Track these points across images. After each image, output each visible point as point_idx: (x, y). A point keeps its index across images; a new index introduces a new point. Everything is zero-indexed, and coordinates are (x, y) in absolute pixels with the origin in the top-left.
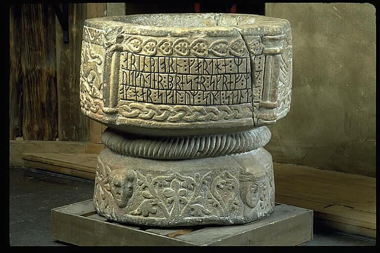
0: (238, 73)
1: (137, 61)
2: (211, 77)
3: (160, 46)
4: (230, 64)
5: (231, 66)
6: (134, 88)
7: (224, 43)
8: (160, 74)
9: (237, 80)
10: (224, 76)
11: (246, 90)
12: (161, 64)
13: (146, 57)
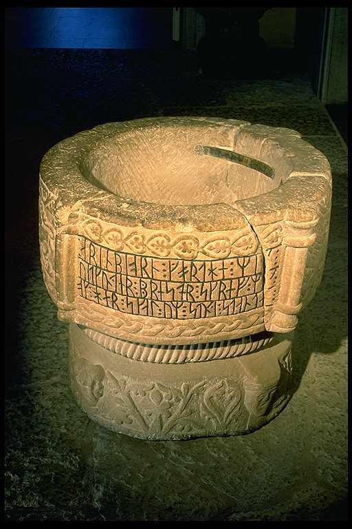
0: (243, 276)
1: (98, 253)
2: (203, 285)
3: (128, 238)
4: (231, 267)
5: (232, 270)
6: (95, 287)
9: (241, 286)
10: (221, 283)
11: (254, 295)
12: (130, 265)
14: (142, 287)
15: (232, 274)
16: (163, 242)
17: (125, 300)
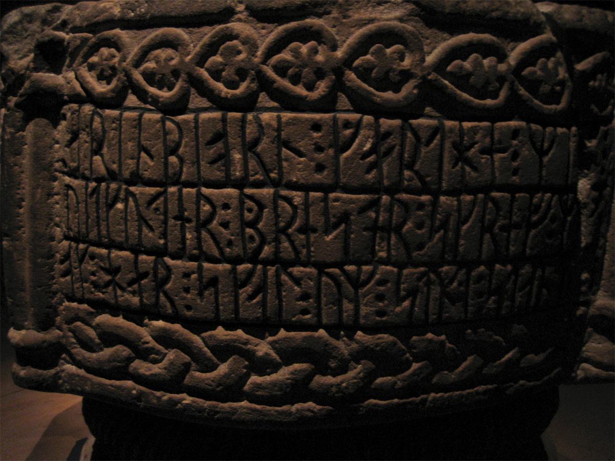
5: (515, 156)
7: (485, 50)
12: (211, 142)
14: (249, 216)
15: (515, 172)
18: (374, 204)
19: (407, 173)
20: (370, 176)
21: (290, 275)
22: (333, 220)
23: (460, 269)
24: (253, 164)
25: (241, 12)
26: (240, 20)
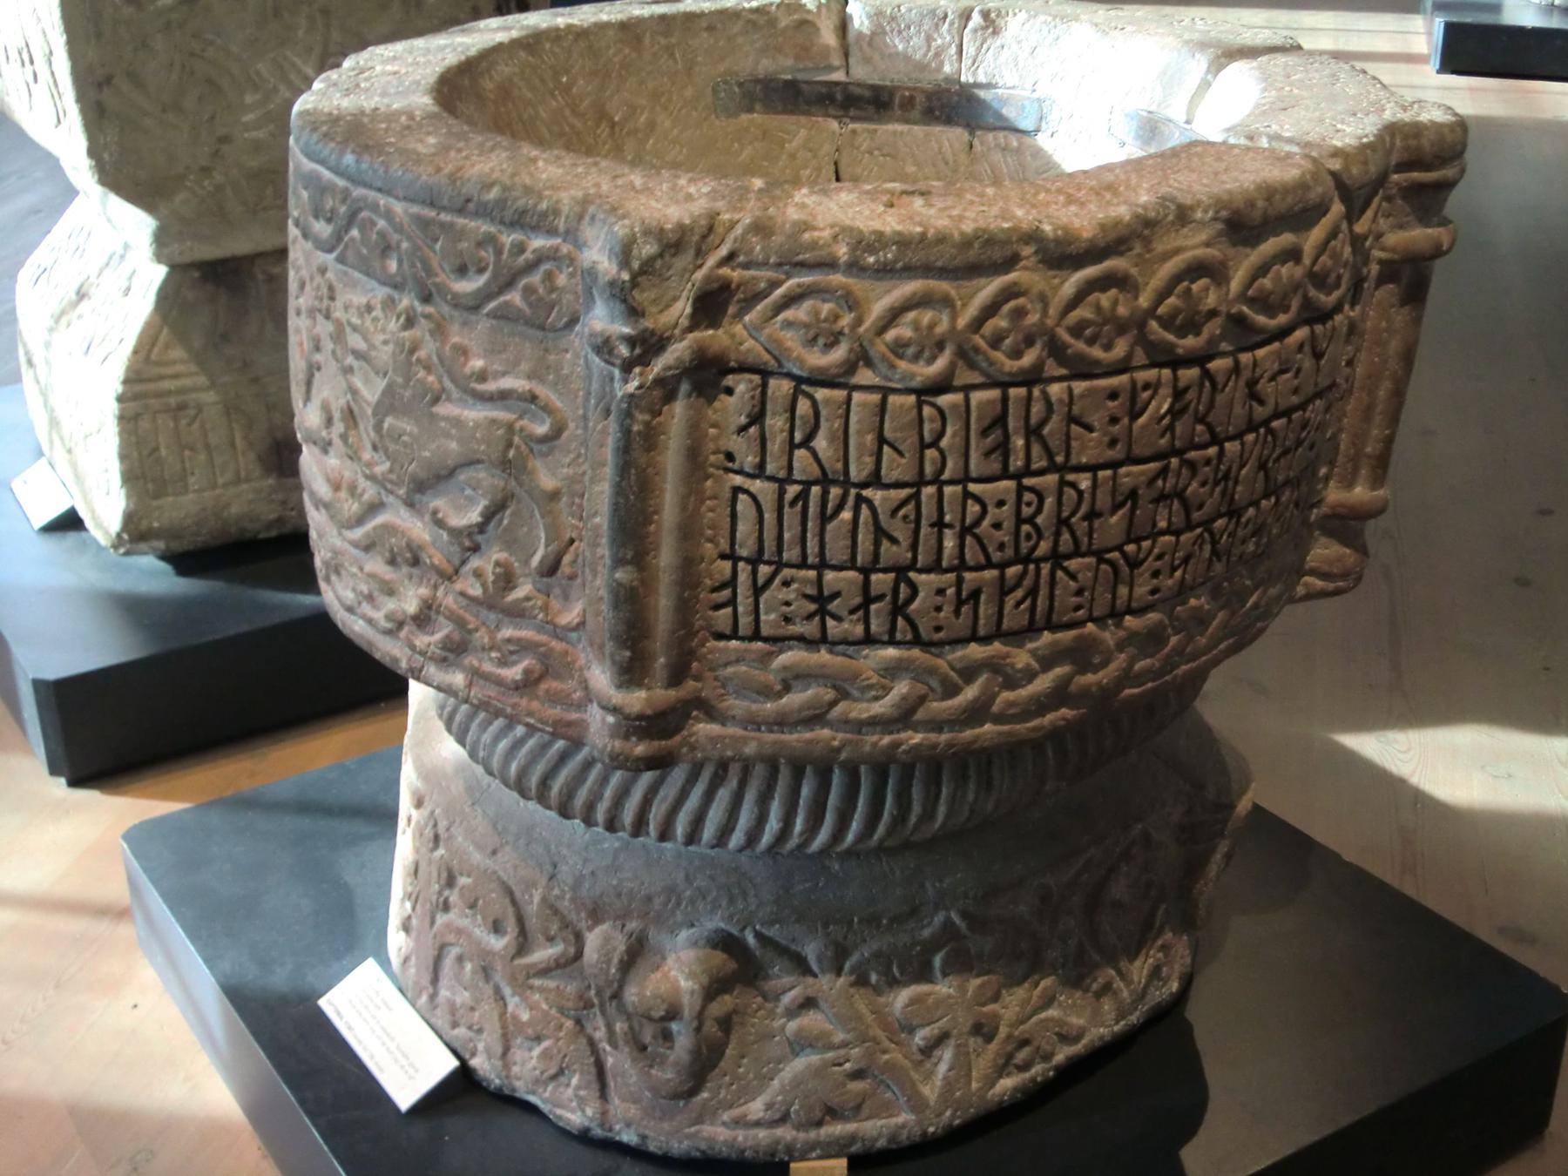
6: (812, 574)
8: (972, 487)
13: (893, 399)
14: (1027, 511)
16: (1115, 303)
17: (951, 591)
18: (1164, 472)
19: (1199, 428)
20: (1163, 441)
21: (1066, 571)
22: (1120, 498)
23: (1230, 519)
24: (1036, 449)
25: (1027, 258)
26: (1025, 268)
